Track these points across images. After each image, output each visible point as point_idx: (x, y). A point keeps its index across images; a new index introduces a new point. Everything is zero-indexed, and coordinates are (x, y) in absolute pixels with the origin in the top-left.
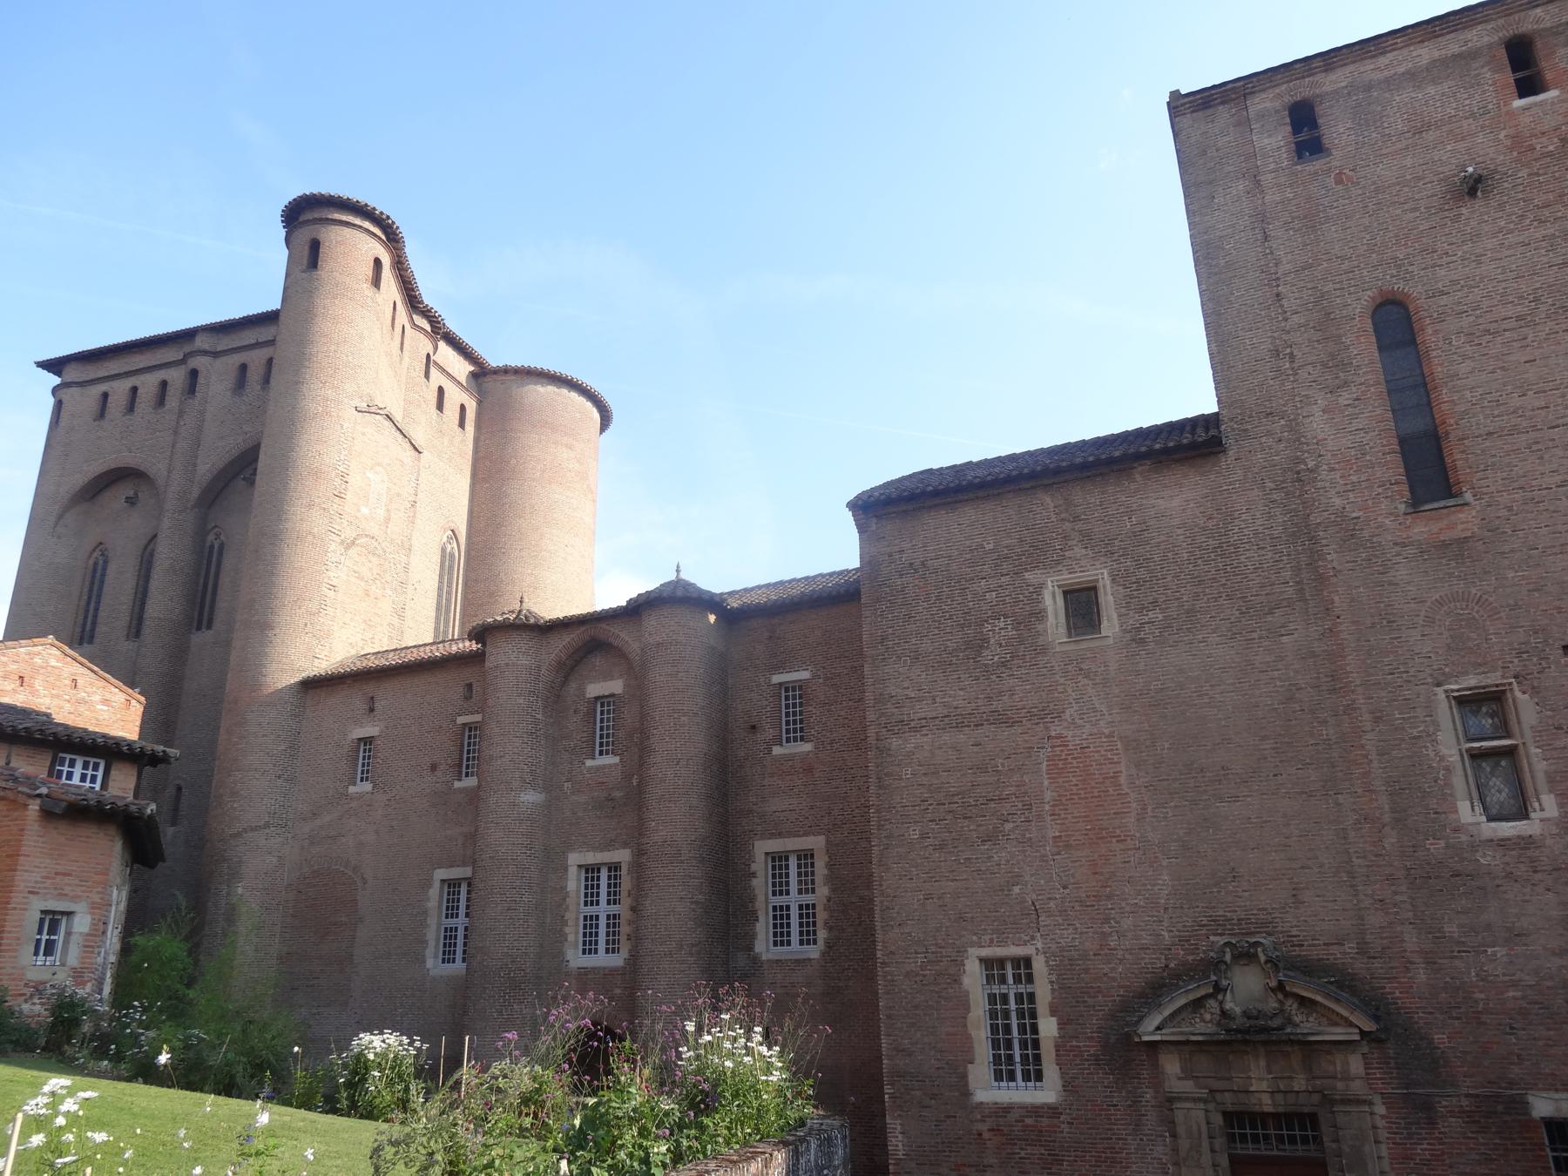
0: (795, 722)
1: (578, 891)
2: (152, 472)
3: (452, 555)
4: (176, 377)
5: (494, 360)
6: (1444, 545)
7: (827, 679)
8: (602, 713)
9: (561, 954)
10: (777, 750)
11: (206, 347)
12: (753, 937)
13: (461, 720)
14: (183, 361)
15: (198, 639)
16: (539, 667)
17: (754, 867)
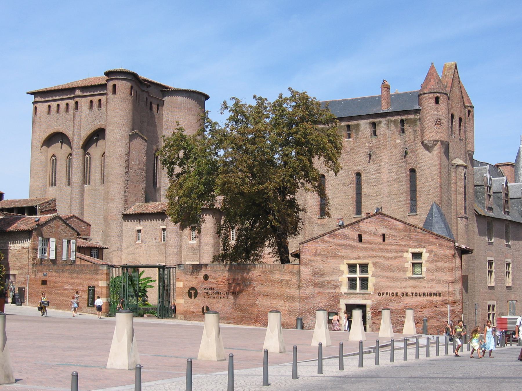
2: (67, 134)
4: (71, 102)
6: (322, 225)
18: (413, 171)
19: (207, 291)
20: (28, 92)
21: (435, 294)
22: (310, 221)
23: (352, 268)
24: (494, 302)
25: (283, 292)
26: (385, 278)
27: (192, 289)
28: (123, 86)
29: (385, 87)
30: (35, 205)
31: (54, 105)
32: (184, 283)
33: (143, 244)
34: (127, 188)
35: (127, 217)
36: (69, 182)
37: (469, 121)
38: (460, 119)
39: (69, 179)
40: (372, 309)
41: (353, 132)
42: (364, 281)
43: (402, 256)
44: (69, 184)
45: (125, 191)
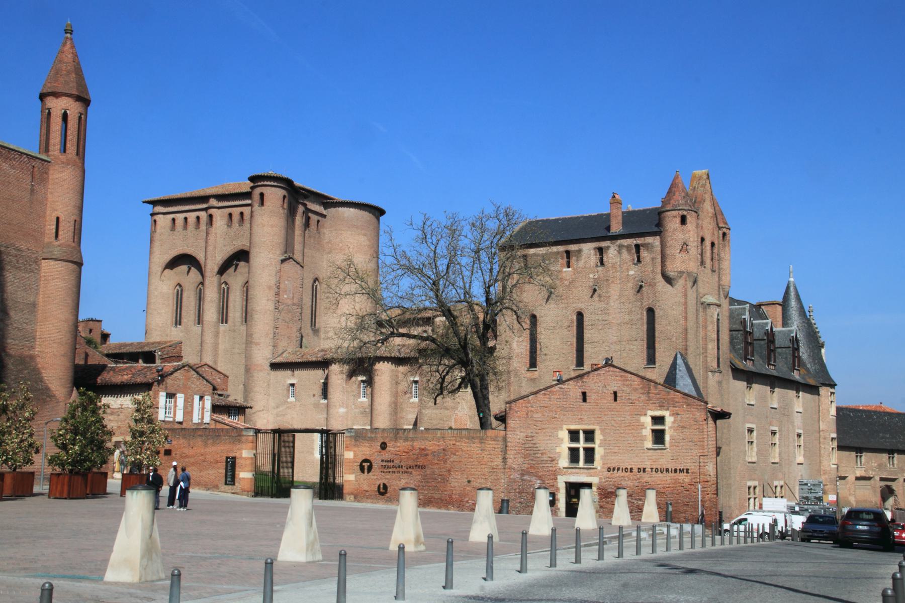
2: (198, 258)
18: (651, 312)
19: (385, 464)
20: (147, 199)
21: (681, 471)
22: (516, 375)
23: (574, 435)
24: (756, 483)
25: (483, 466)
26: (616, 449)
27: (366, 461)
28: (275, 195)
29: (615, 201)
30: (153, 350)
31: (180, 217)
32: (355, 452)
33: (298, 404)
34: (277, 328)
35: (275, 366)
36: (199, 320)
37: (724, 246)
38: (713, 244)
39: (199, 316)
40: (599, 488)
41: (573, 260)
42: (590, 455)
43: (639, 421)
44: (199, 323)
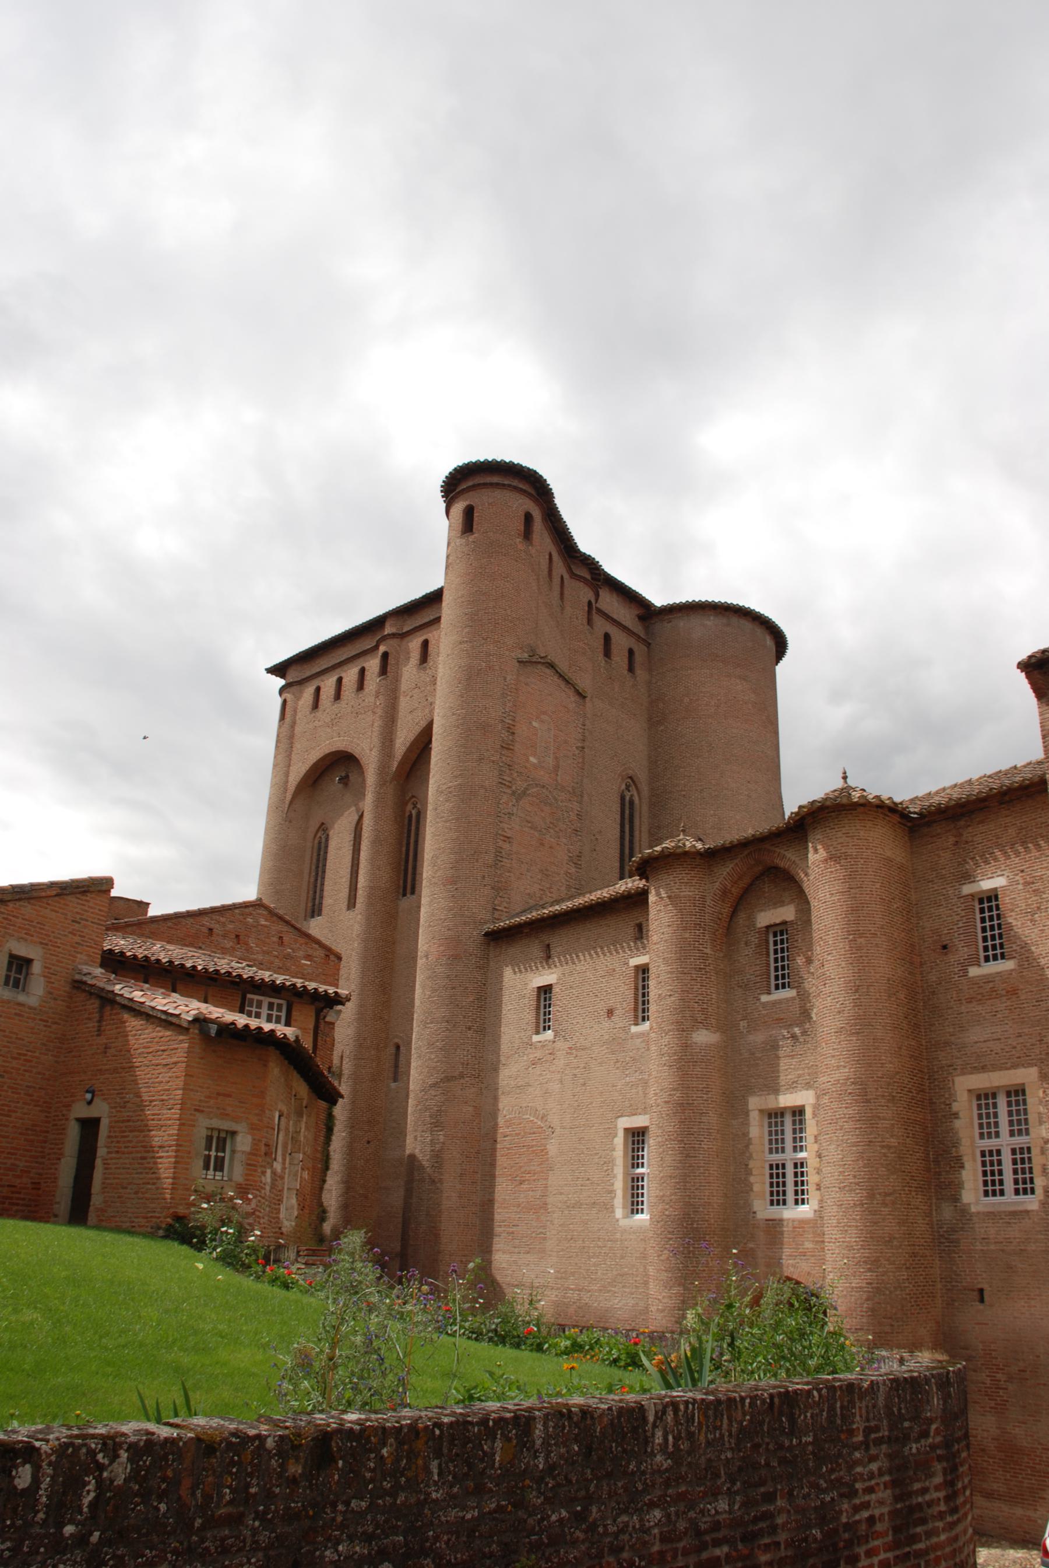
0: (993, 937)
1: (761, 1137)
2: (356, 752)
3: (632, 803)
4: (373, 664)
5: (659, 600)
7: (1027, 884)
8: (775, 943)
9: (748, 1205)
10: (974, 971)
11: (394, 630)
12: (960, 1186)
13: (635, 961)
14: (376, 647)
15: (405, 903)
16: (703, 897)
17: (955, 1107)
33: (560, 1044)
45: (498, 852)
